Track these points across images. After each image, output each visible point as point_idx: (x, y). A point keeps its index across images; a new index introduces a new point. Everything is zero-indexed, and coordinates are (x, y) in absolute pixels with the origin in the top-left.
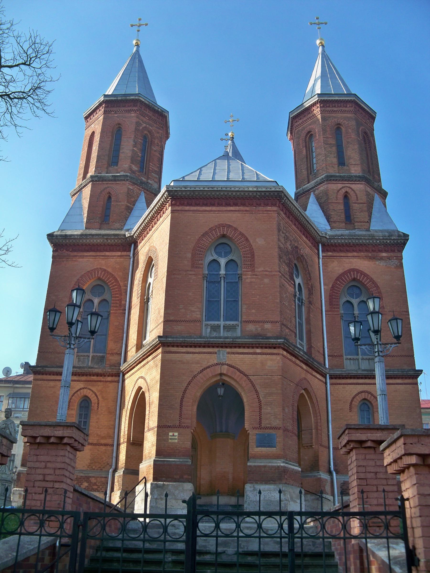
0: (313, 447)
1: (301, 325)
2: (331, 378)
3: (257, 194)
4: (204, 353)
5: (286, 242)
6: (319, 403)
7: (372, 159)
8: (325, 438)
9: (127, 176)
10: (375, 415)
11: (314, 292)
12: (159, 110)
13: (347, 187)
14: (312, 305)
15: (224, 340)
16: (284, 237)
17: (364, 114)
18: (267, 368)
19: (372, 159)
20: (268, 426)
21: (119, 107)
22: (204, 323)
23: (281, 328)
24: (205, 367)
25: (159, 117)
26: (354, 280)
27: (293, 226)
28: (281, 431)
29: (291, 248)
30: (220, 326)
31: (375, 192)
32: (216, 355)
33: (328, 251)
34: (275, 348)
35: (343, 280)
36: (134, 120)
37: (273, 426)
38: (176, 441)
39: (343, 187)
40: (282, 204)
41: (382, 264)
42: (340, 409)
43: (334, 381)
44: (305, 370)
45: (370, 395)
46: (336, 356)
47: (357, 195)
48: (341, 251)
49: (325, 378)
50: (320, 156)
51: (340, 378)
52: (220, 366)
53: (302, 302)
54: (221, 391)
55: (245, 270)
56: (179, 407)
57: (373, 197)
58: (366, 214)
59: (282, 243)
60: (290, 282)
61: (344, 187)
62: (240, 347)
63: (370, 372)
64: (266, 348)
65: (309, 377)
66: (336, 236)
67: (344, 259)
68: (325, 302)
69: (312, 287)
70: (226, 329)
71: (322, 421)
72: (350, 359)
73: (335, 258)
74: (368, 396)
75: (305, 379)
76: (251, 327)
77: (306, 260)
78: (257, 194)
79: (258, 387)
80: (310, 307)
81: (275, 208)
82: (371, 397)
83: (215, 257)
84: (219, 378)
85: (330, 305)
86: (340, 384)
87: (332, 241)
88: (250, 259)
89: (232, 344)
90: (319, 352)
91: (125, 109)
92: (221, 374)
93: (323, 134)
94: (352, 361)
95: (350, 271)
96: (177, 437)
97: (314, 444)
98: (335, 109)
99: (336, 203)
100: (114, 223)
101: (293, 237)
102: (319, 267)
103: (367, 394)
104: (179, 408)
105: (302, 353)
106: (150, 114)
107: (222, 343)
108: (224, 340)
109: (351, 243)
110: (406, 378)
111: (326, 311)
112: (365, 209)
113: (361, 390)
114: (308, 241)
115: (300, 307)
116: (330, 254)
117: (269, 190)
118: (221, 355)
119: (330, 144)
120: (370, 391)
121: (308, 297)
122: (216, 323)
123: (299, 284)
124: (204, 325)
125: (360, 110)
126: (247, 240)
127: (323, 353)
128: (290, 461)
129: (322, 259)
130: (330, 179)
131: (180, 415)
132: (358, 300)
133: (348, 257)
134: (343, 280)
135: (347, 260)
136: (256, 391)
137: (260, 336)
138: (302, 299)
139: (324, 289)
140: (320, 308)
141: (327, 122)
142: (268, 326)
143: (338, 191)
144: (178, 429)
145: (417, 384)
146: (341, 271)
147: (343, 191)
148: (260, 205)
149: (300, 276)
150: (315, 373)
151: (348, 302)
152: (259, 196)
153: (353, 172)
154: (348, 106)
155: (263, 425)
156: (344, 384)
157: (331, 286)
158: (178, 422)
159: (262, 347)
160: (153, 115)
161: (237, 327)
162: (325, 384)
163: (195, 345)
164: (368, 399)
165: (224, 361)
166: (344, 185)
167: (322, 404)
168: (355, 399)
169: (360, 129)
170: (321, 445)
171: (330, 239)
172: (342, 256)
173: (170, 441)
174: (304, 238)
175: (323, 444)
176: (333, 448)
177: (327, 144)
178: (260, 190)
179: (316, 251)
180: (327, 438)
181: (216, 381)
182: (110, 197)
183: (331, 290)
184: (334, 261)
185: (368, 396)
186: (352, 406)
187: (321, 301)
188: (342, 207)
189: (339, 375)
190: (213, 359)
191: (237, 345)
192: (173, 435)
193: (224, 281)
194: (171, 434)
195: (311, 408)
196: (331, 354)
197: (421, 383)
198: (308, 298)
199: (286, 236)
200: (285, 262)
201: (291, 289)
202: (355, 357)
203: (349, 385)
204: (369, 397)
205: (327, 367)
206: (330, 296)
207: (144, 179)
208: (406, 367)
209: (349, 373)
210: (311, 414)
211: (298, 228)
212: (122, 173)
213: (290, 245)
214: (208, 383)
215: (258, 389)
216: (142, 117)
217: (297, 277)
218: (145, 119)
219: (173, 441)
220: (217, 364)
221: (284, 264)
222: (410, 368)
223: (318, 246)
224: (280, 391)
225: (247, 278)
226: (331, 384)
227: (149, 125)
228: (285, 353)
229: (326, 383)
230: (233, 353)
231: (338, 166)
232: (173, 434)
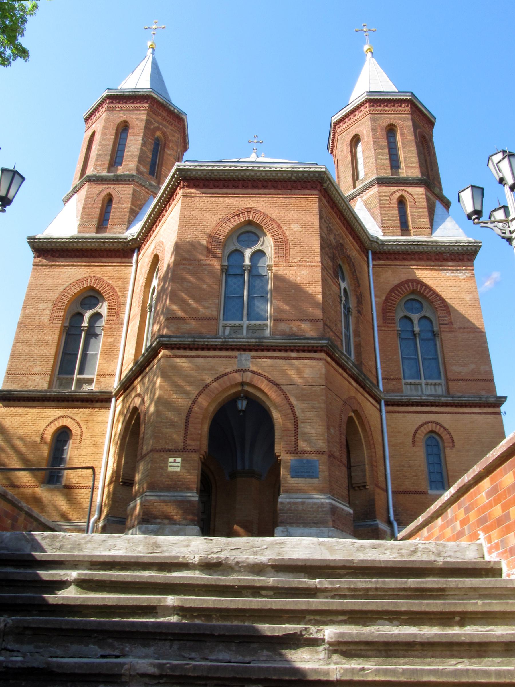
0: (367, 487)
1: (348, 337)
2: (387, 404)
3: (292, 174)
4: (220, 357)
5: (329, 234)
6: (373, 433)
7: (431, 165)
8: (382, 479)
10: (446, 451)
11: (363, 302)
13: (403, 190)
14: (361, 315)
15: (247, 340)
16: (327, 227)
17: (422, 117)
19: (431, 165)
24: (221, 374)
26: (413, 292)
27: (338, 220)
29: (336, 242)
30: (242, 327)
32: (236, 360)
33: (380, 259)
35: (399, 292)
38: (178, 469)
39: (397, 191)
40: (324, 189)
43: (391, 408)
45: (438, 427)
47: (414, 200)
48: (396, 259)
49: (380, 404)
50: (369, 160)
52: (242, 373)
53: (349, 311)
54: (242, 405)
55: (277, 259)
56: (185, 424)
59: (324, 232)
61: (399, 190)
62: (268, 350)
63: (437, 398)
65: (360, 397)
67: (401, 269)
68: (377, 316)
69: (361, 295)
70: (251, 331)
71: (377, 456)
72: (411, 384)
73: (389, 267)
74: (436, 427)
75: (355, 398)
77: (353, 263)
78: (292, 174)
80: (359, 317)
82: (440, 429)
84: (239, 388)
85: (383, 320)
87: (385, 248)
88: (283, 247)
89: (258, 346)
90: (371, 372)
92: (242, 384)
93: (373, 135)
94: (413, 387)
95: (407, 282)
96: (179, 464)
97: (368, 484)
99: (389, 207)
101: (337, 231)
102: (369, 276)
103: (434, 425)
105: (351, 365)
107: (245, 345)
108: (247, 340)
109: (409, 250)
110: (485, 407)
111: (378, 327)
113: (427, 420)
114: (355, 243)
115: (347, 316)
116: (382, 262)
118: (243, 359)
119: (382, 145)
120: (439, 422)
121: (356, 305)
123: (345, 289)
125: (417, 111)
126: (279, 226)
127: (375, 375)
129: (373, 268)
130: (381, 182)
133: (404, 266)
134: (399, 292)
135: (404, 270)
137: (294, 335)
138: (349, 308)
139: (376, 301)
140: (371, 322)
141: (378, 122)
143: (392, 194)
144: (181, 453)
145: (499, 414)
146: (396, 282)
147: (398, 194)
149: (346, 280)
150: (366, 395)
151: (406, 317)
152: (296, 177)
154: (403, 105)
156: (403, 412)
157: (384, 298)
158: (182, 444)
161: (264, 328)
162: (379, 412)
163: (208, 348)
164: (437, 431)
167: (377, 436)
168: (419, 431)
170: (377, 486)
171: (382, 244)
174: (351, 238)
175: (379, 485)
177: (378, 145)
179: (366, 259)
180: (384, 479)
181: (235, 393)
183: (384, 303)
184: (387, 271)
185: (436, 427)
186: (416, 439)
187: (372, 314)
189: (398, 402)
191: (265, 347)
192: (175, 462)
193: (249, 275)
195: (362, 438)
196: (386, 376)
197: (505, 413)
198: (357, 307)
200: (327, 254)
201: (335, 288)
202: (417, 381)
203: (410, 414)
204: (437, 429)
206: (383, 309)
208: (483, 393)
209: (410, 399)
210: (362, 445)
213: (334, 239)
214: (226, 395)
219: (174, 469)
221: (327, 256)
223: (368, 253)
226: (387, 412)
229: (380, 411)
231: (391, 169)
232: (175, 460)
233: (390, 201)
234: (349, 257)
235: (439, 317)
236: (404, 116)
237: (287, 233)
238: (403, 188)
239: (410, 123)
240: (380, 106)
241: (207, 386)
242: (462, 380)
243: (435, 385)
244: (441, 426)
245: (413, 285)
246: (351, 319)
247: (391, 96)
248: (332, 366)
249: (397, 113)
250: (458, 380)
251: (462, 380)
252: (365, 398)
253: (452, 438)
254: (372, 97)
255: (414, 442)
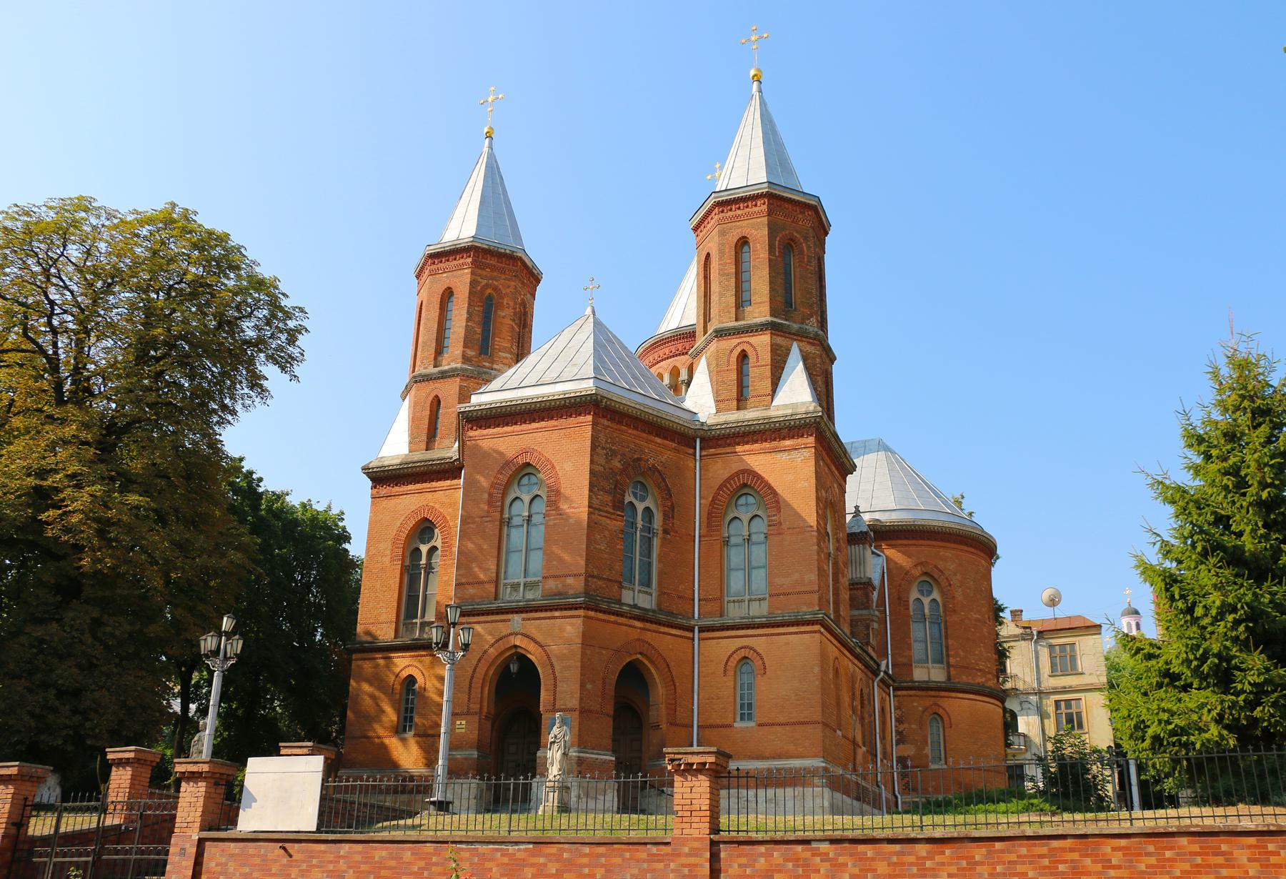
4: (497, 621)
9: (456, 369)
12: (508, 251)
18: (566, 635)
20: (563, 707)
21: (448, 261)
22: (503, 582)
23: (586, 581)
25: (508, 262)
28: (577, 713)
31: (796, 340)
34: (576, 609)
36: (467, 279)
37: (568, 707)
38: (463, 731)
41: (784, 456)
42: (712, 674)
44: (640, 628)
46: (711, 600)
49: (691, 629)
51: (713, 631)
53: (654, 533)
54: (514, 668)
55: (548, 508)
57: (788, 351)
58: (768, 383)
60: (612, 514)
62: (536, 611)
64: (566, 609)
66: (717, 425)
72: (734, 601)
76: (552, 584)
77: (658, 471)
79: (554, 660)
81: (589, 418)
83: (518, 494)
84: (513, 651)
86: (713, 638)
91: (455, 263)
92: (516, 647)
95: (737, 474)
98: (739, 212)
100: (443, 440)
104: (467, 691)
106: (493, 262)
110: (803, 625)
111: (700, 537)
112: (768, 373)
113: (740, 645)
116: (712, 451)
117: (578, 394)
121: (661, 524)
122: (516, 581)
123: (647, 509)
124: (502, 585)
126: (553, 467)
128: (593, 749)
129: (701, 460)
131: (469, 699)
132: (750, 515)
136: (552, 665)
142: (570, 581)
143: (732, 351)
146: (727, 475)
147: (739, 349)
148: (571, 416)
150: (663, 629)
151: (736, 518)
153: (757, 315)
154: (759, 203)
155: (557, 707)
157: (710, 499)
159: (561, 609)
160: (498, 262)
165: (517, 630)
166: (739, 341)
169: (778, 238)
172: (728, 453)
173: (457, 731)
174: (658, 440)
176: (698, 727)
178: (567, 396)
182: (439, 402)
188: (734, 376)
190: (503, 629)
194: (458, 722)
199: (611, 450)
200: (603, 489)
204: (750, 654)
205: (696, 616)
207: (487, 364)
211: (643, 431)
212: (453, 365)
215: (555, 663)
216: (480, 271)
217: (643, 499)
218: (484, 273)
219: (460, 730)
220: (511, 634)
222: (810, 610)
224: (579, 664)
225: (550, 520)
227: (492, 279)
228: (592, 613)
229: (693, 639)
230: (529, 619)
233: (728, 361)
234: (653, 469)
235: (769, 516)
236: (759, 220)
237: (560, 474)
238: (745, 339)
239: (765, 232)
240: (731, 210)
241: (485, 652)
242: (784, 594)
243: (760, 600)
244: (755, 651)
245: (744, 478)
246: (656, 542)
247: (744, 192)
248: (598, 619)
249: (751, 216)
250: (778, 595)
251: (784, 594)
252: (664, 633)
253: (764, 663)
254: (720, 199)
255: (725, 671)
